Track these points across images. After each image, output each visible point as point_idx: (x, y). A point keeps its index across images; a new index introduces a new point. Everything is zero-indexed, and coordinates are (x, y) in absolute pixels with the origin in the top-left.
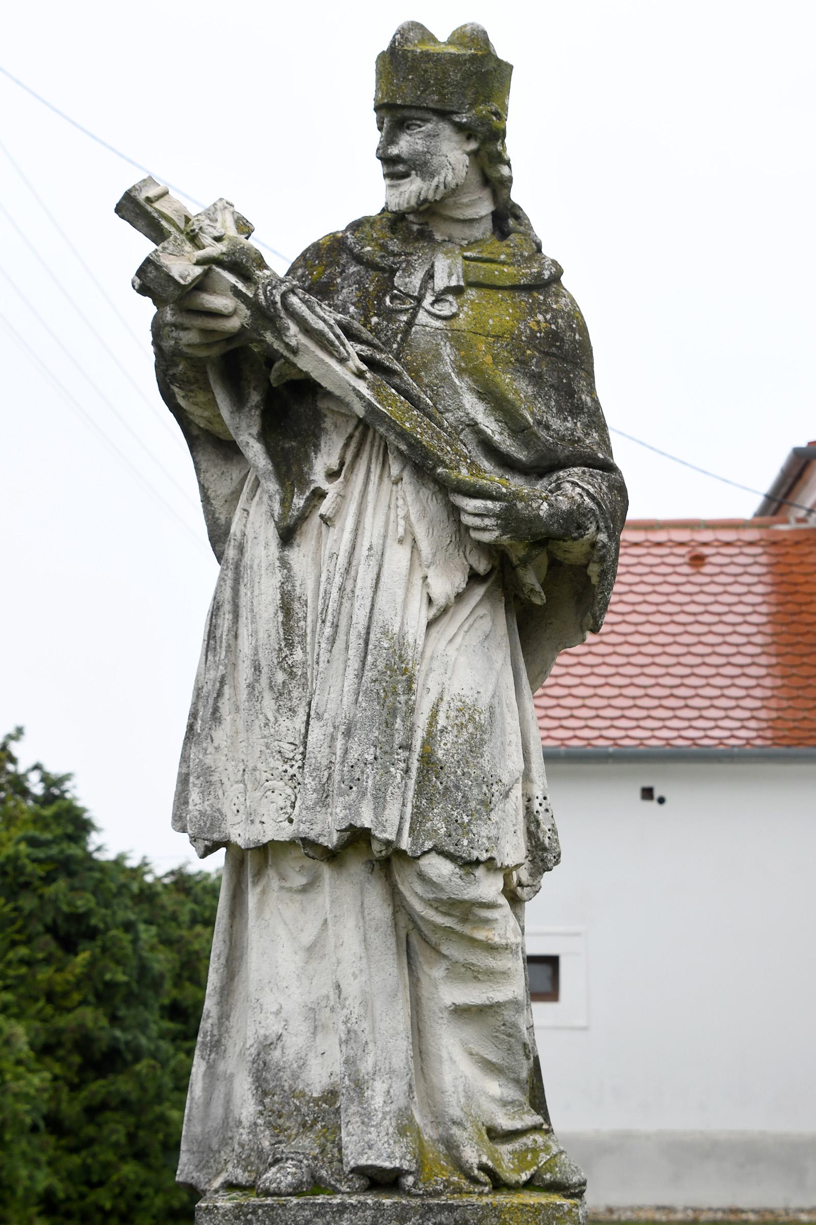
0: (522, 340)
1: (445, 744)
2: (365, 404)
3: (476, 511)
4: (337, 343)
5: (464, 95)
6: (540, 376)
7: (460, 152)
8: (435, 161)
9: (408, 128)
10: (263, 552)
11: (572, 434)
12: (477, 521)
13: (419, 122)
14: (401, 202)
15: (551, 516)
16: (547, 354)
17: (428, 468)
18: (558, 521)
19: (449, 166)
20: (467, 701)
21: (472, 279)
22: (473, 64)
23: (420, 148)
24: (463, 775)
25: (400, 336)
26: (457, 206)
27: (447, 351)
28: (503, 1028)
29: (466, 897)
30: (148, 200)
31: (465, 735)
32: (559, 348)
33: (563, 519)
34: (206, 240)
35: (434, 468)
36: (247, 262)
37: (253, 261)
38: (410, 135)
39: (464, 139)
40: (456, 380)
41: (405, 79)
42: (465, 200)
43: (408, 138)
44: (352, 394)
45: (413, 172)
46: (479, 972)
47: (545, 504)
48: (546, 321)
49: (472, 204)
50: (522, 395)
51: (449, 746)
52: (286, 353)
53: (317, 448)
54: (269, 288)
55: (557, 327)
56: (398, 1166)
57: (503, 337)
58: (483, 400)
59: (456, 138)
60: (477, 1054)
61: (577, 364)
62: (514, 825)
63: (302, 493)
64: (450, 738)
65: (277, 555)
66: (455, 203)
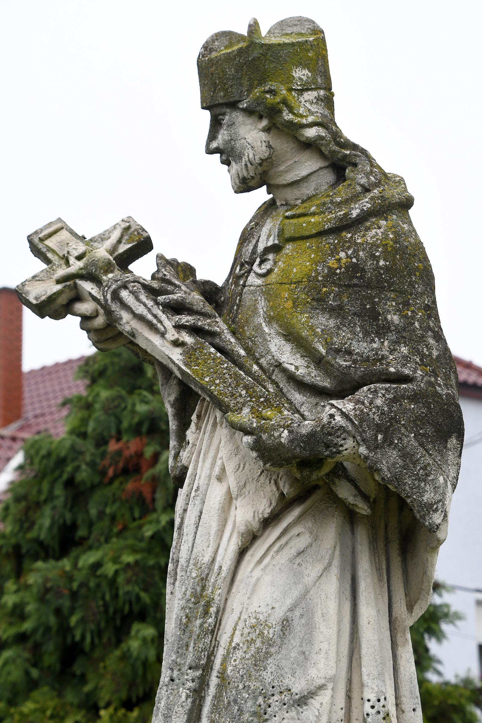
0: (318, 281)
1: (235, 660)
4: (155, 321)
5: (241, 85)
6: (341, 307)
7: (256, 131)
11: (377, 354)
13: (221, 117)
15: (291, 441)
16: (349, 286)
18: (298, 445)
19: (249, 146)
20: (261, 617)
21: (287, 235)
22: (241, 57)
23: (226, 138)
24: (244, 688)
25: (238, 298)
27: (262, 305)
31: (253, 650)
32: (361, 278)
33: (303, 442)
34: (72, 260)
36: (95, 271)
37: (100, 269)
39: (255, 118)
40: (266, 330)
42: (282, 168)
47: (286, 432)
48: (347, 256)
50: (319, 330)
51: (237, 662)
54: (106, 288)
55: (358, 260)
57: (302, 282)
59: (249, 121)
61: (383, 288)
64: (239, 654)
66: (275, 173)
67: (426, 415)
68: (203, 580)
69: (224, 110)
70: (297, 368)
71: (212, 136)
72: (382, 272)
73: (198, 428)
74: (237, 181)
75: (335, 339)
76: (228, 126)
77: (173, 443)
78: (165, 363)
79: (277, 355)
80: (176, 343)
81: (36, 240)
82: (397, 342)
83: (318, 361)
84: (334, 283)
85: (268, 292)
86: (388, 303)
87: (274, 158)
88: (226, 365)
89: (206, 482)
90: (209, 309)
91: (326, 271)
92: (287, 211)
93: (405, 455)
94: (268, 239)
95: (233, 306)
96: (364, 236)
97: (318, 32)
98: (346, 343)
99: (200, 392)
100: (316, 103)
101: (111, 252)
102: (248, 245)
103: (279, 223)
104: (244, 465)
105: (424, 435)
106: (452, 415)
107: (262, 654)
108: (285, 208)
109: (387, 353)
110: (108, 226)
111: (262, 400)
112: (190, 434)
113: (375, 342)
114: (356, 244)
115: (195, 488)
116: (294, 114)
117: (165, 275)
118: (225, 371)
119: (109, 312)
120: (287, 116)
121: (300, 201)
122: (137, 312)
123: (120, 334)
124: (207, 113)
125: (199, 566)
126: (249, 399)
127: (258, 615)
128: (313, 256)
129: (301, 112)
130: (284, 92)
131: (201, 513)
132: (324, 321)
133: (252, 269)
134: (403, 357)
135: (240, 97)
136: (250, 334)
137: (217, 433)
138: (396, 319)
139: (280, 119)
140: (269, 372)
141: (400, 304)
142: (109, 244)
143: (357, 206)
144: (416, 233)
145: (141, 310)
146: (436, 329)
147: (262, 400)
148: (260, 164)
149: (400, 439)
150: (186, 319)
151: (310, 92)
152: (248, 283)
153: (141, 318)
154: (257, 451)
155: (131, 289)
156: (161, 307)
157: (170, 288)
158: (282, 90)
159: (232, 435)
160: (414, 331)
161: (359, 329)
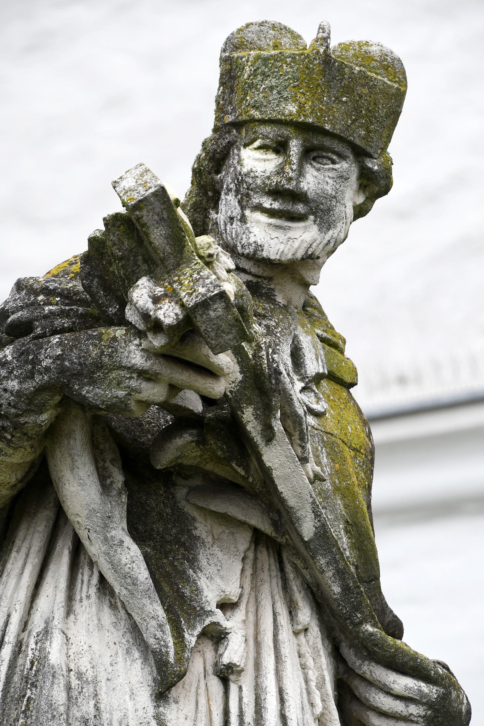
2: (319, 524)
3: (406, 694)
9: (314, 159)
10: (130, 705)
12: (399, 707)
13: (335, 157)
14: (286, 251)
17: (352, 623)
23: (329, 189)
35: (361, 623)
38: (318, 170)
41: (338, 99)
43: (316, 173)
44: (309, 507)
45: (312, 217)
52: (258, 439)
53: (193, 562)
63: (194, 627)
65: (151, 711)
69: (348, 153)
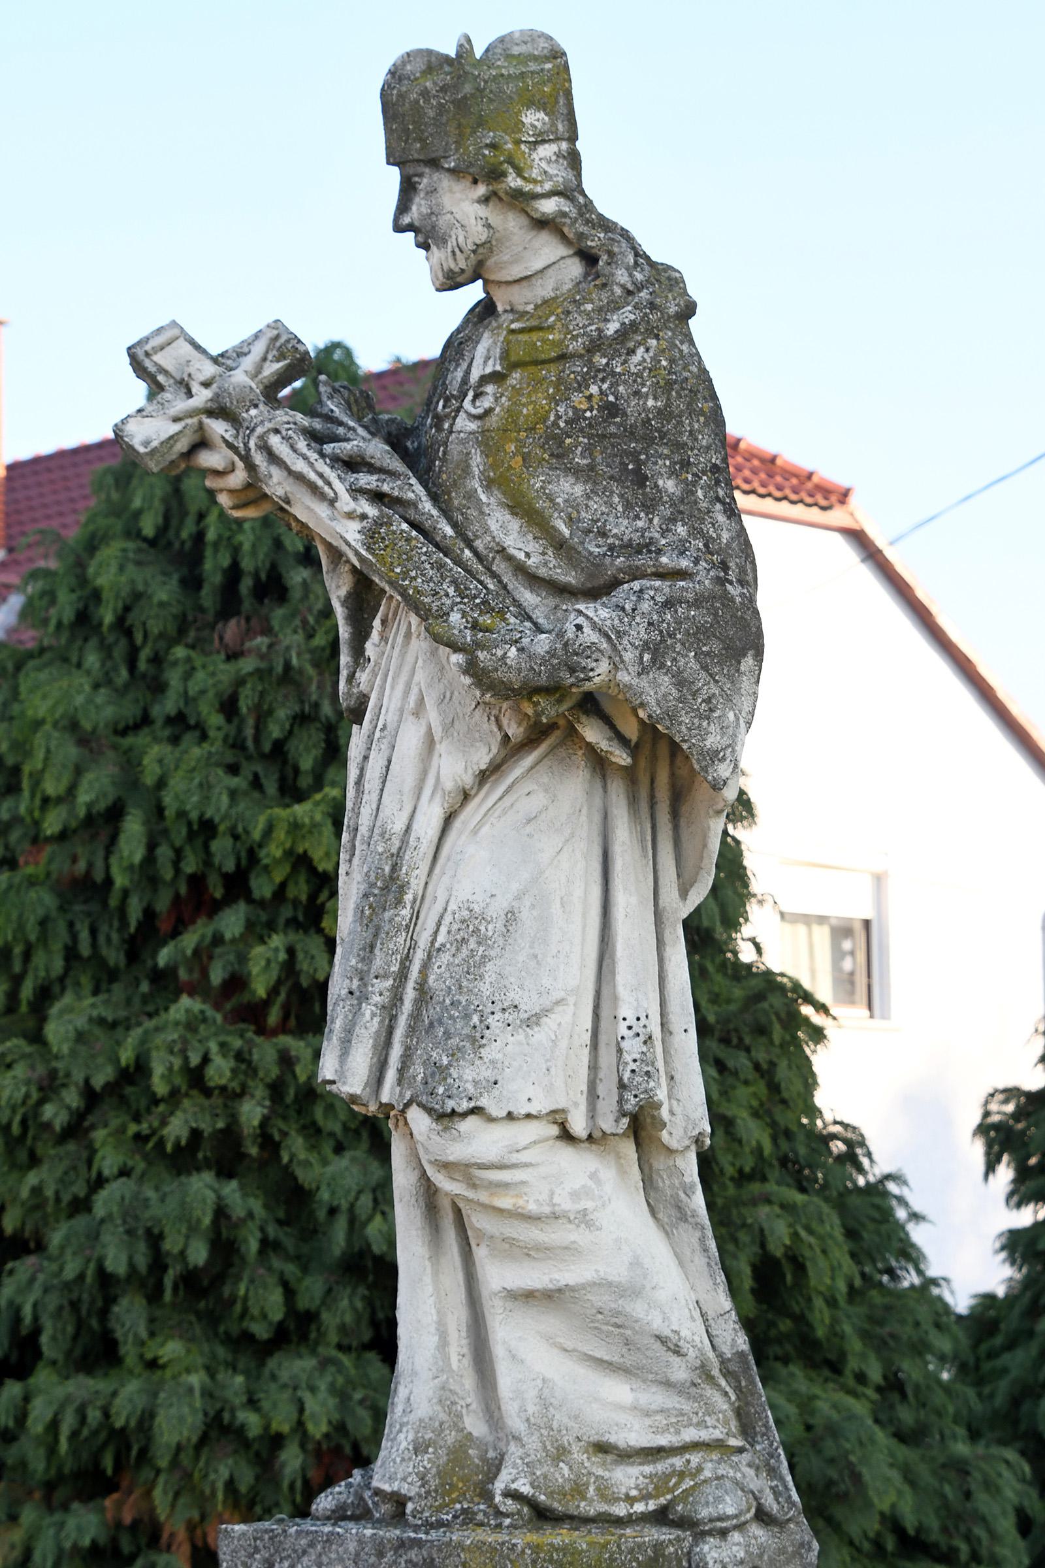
4: (320, 483)
6: (592, 468)
7: (467, 203)
8: (441, 222)
11: (643, 536)
13: (416, 179)
19: (458, 225)
20: (477, 909)
21: (513, 358)
23: (424, 210)
26: (500, 266)
27: (477, 460)
28: (600, 1317)
29: (451, 1158)
30: (147, 354)
39: (467, 182)
40: (483, 498)
46: (529, 1249)
47: (513, 649)
49: (517, 259)
50: (559, 500)
51: (443, 969)
55: (616, 399)
56: (395, 1489)
58: (516, 514)
60: (574, 1350)
62: (547, 1061)
64: (445, 958)
67: (712, 626)
68: (396, 860)
70: (528, 555)
71: (403, 206)
72: (651, 416)
73: (384, 638)
74: (440, 275)
75: (583, 514)
76: (427, 193)
77: (345, 659)
78: (335, 544)
79: (500, 535)
80: (350, 516)
81: (140, 353)
82: (673, 520)
83: (560, 545)
84: (581, 430)
85: (487, 441)
86: (660, 462)
87: (494, 243)
88: (425, 549)
89: (396, 718)
90: (397, 465)
91: (571, 414)
92: (512, 322)
93: (681, 682)
94: (485, 362)
95: (433, 462)
96: (625, 362)
97: (557, 55)
98: (599, 520)
99: (387, 588)
100: (557, 161)
101: (254, 376)
102: (455, 369)
103: (501, 339)
104: (452, 693)
105: (708, 654)
106: (749, 625)
107: (477, 958)
108: (511, 316)
109: (657, 535)
110: (247, 333)
111: (478, 601)
112: (370, 648)
113: (640, 519)
114: (614, 374)
115: (380, 726)
116: (524, 178)
117: (332, 411)
118: (424, 558)
119: (251, 467)
120: (513, 181)
121: (532, 306)
122: (293, 468)
123: (265, 496)
124: (396, 170)
125: (387, 836)
126: (459, 600)
127: (472, 906)
128: (551, 391)
129: (534, 176)
130: (510, 146)
131: (389, 762)
132: (568, 488)
133: (462, 407)
134: (680, 541)
135: (445, 151)
136: (460, 504)
137: (411, 646)
138: (669, 485)
139: (503, 186)
140: (487, 560)
141: (676, 463)
142: (248, 363)
143: (615, 317)
144: (700, 358)
145: (300, 466)
146: (728, 500)
147: (478, 601)
148: (474, 252)
149: (675, 659)
150: (366, 480)
151: (547, 146)
152: (457, 427)
153: (299, 477)
154: (471, 676)
155: (284, 433)
156: (328, 461)
157: (341, 431)
158: (505, 143)
159: (434, 653)
160: (696, 502)
161: (616, 499)
